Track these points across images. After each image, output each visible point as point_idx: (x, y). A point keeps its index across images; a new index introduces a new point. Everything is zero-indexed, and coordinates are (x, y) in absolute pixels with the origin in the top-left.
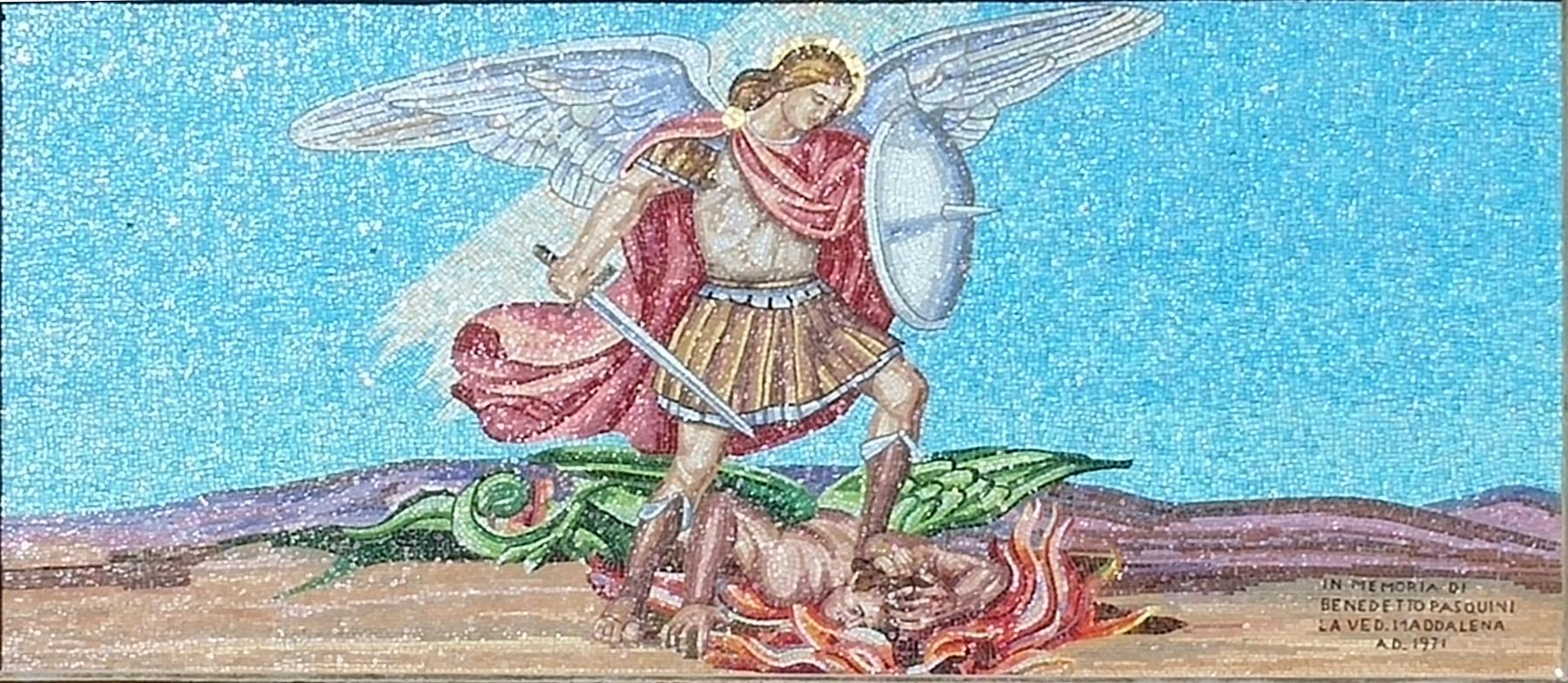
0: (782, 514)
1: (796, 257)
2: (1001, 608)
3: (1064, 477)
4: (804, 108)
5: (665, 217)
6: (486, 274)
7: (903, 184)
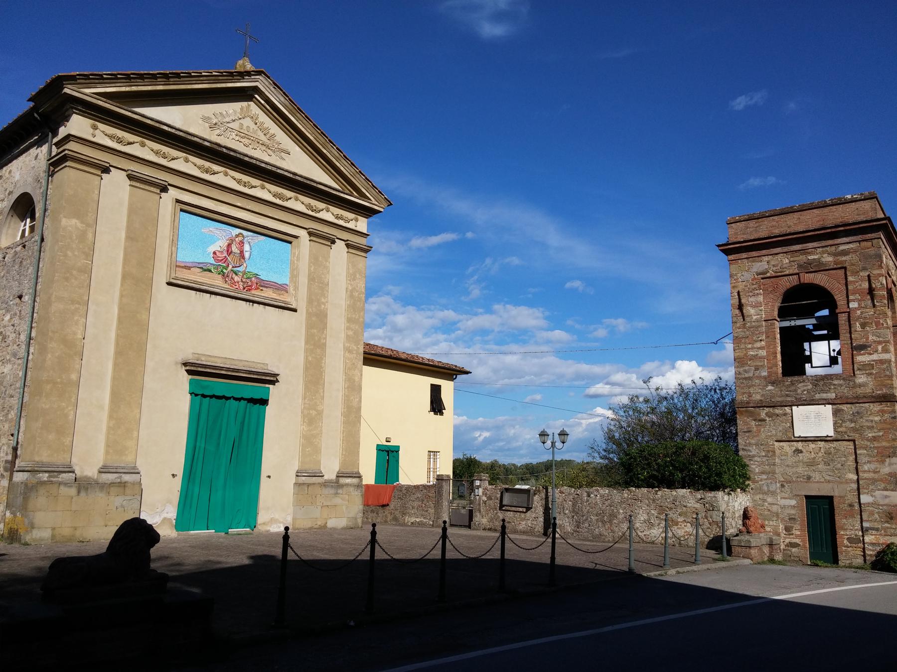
2: (251, 286)
5: (229, 246)
6: (215, 247)
7: (247, 247)
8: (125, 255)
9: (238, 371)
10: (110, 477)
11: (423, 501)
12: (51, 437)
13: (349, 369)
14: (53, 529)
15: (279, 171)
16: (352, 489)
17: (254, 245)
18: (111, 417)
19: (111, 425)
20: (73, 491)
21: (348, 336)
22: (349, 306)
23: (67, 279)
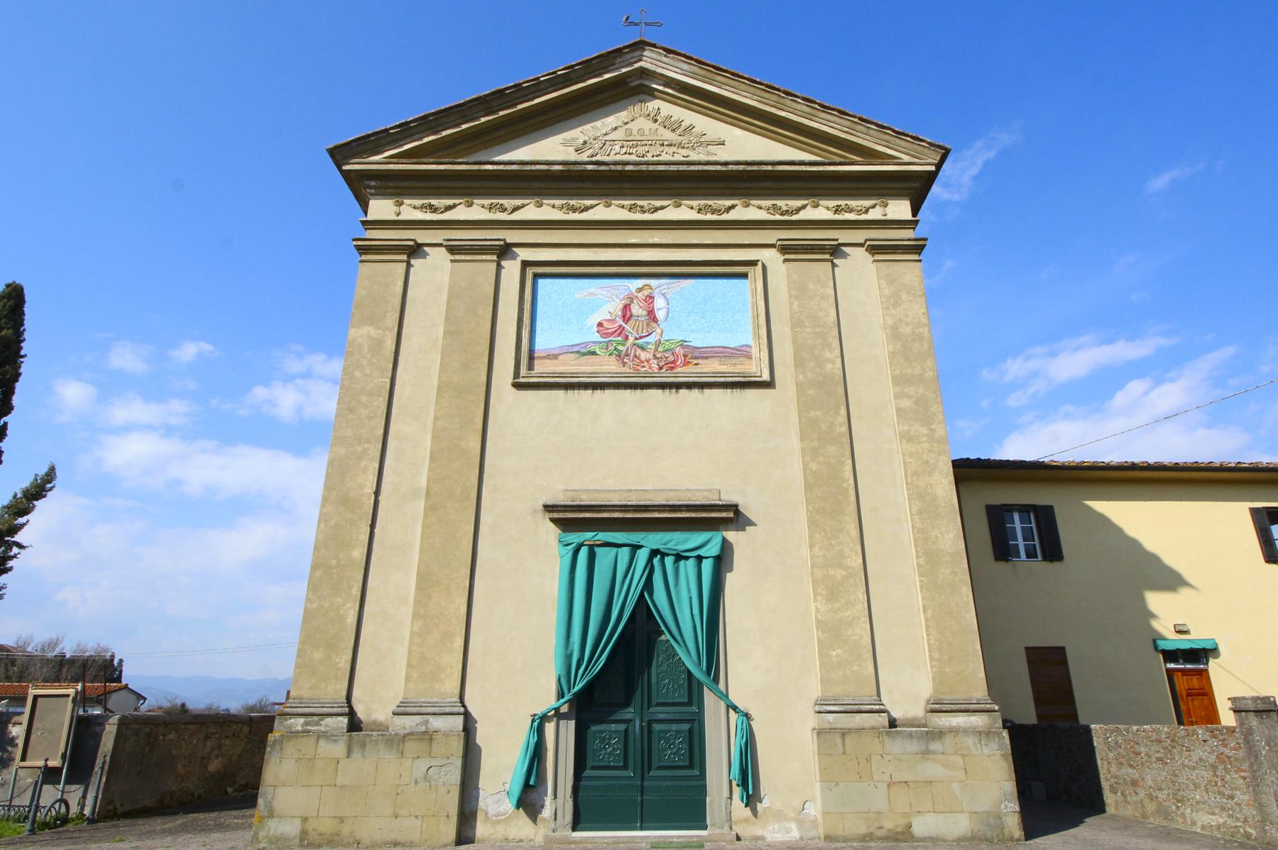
0: (643, 349)
1: (645, 313)
3: (682, 344)
4: (646, 293)
5: (626, 308)
6: (602, 315)
7: (659, 303)
8: (442, 358)
9: (646, 508)
10: (409, 723)
11: (1214, 767)
12: (318, 655)
13: (916, 474)
14: (305, 820)
15: (692, 168)
16: (970, 741)
17: (672, 297)
18: (416, 615)
19: (416, 629)
20: (339, 749)
21: (900, 411)
22: (892, 355)
23: (352, 411)
